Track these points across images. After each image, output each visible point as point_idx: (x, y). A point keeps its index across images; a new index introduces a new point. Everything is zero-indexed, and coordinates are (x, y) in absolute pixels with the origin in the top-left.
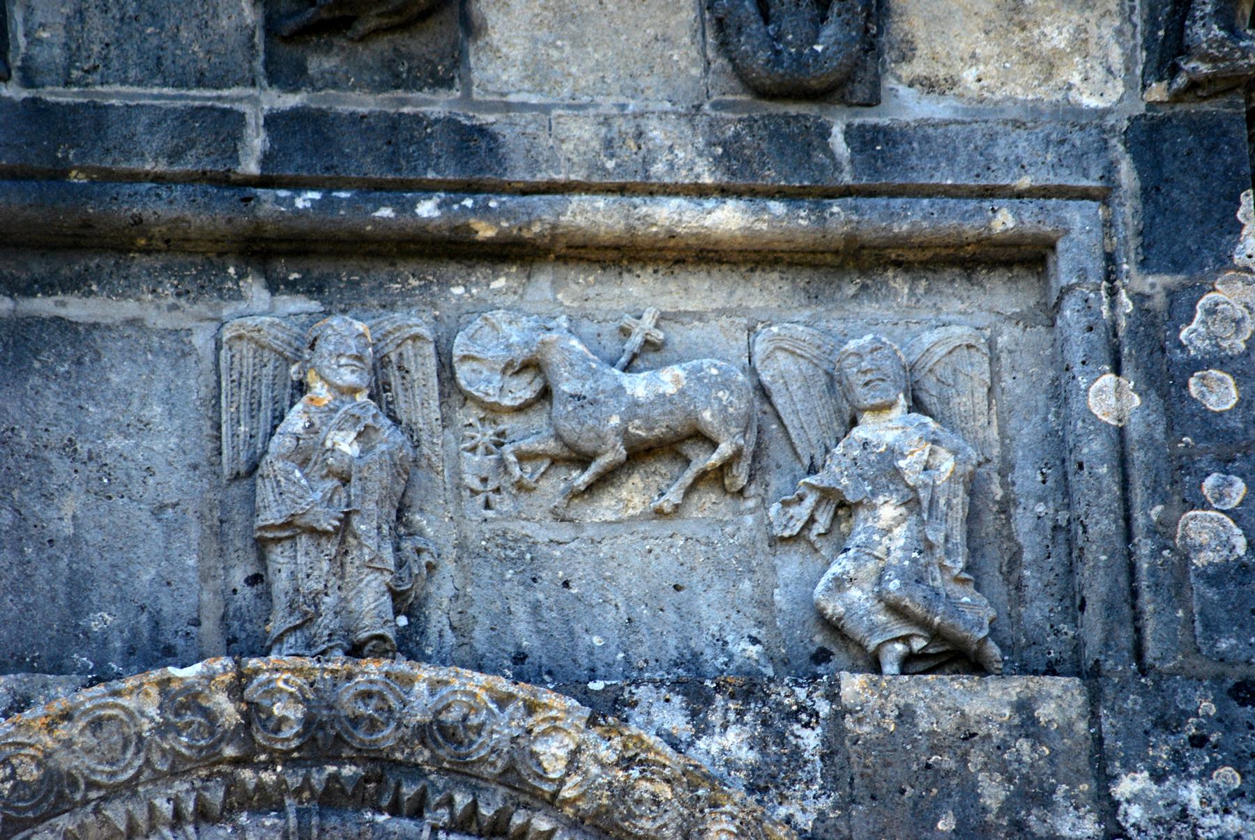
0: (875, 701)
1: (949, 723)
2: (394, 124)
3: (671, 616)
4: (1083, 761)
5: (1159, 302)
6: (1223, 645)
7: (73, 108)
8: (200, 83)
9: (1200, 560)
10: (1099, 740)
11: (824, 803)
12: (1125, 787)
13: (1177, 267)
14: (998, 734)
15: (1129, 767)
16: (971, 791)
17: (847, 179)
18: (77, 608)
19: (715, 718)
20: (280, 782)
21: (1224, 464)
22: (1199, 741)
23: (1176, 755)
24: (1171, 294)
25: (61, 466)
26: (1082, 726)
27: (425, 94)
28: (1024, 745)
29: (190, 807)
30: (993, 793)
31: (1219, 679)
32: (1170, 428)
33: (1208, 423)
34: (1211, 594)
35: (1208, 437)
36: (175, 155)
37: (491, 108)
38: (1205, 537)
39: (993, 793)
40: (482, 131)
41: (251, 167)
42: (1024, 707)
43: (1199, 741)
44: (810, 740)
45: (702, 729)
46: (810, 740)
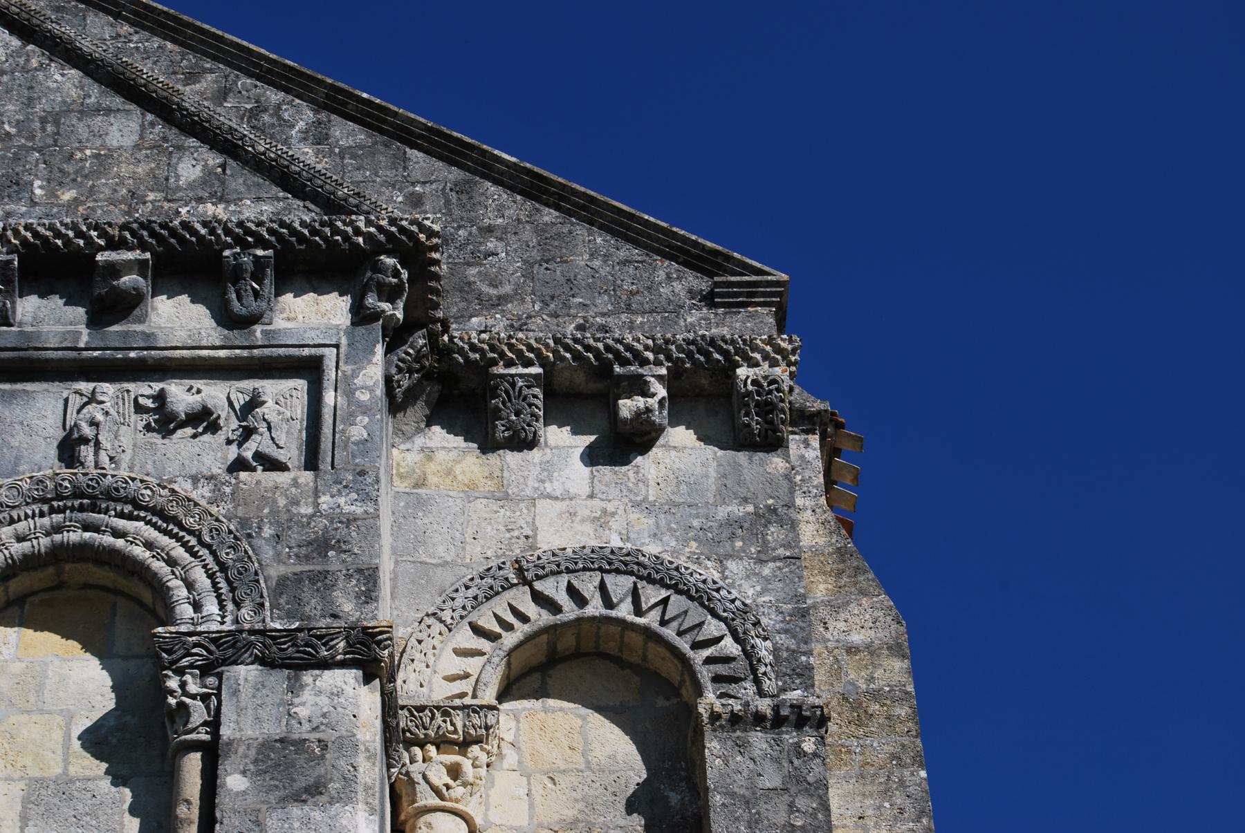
0: (249, 479)
1: (271, 484)
2: (127, 333)
3: (196, 462)
4: (310, 494)
5: (349, 373)
6: (357, 461)
7: (32, 332)
8: (71, 325)
9: (353, 439)
10: (316, 488)
11: (230, 506)
12: (323, 499)
13: (356, 363)
14: (285, 487)
15: (324, 494)
16: (275, 501)
17: (260, 343)
18: (16, 465)
19: (200, 485)
20: (65, 504)
21: (364, 413)
22: (346, 487)
23: (339, 491)
24: (353, 371)
25: (17, 427)
26: (312, 484)
27: (137, 325)
28: (293, 490)
29: (37, 512)
30: (282, 502)
31: (354, 470)
32: (349, 405)
33: (360, 404)
34: (355, 448)
35: (359, 407)
36: (61, 342)
37: (156, 328)
38: (355, 433)
39: (282, 502)
40: (153, 333)
41: (82, 345)
42: (295, 480)
43: (346, 487)
44: (228, 490)
45: (195, 488)
46: (228, 490)
